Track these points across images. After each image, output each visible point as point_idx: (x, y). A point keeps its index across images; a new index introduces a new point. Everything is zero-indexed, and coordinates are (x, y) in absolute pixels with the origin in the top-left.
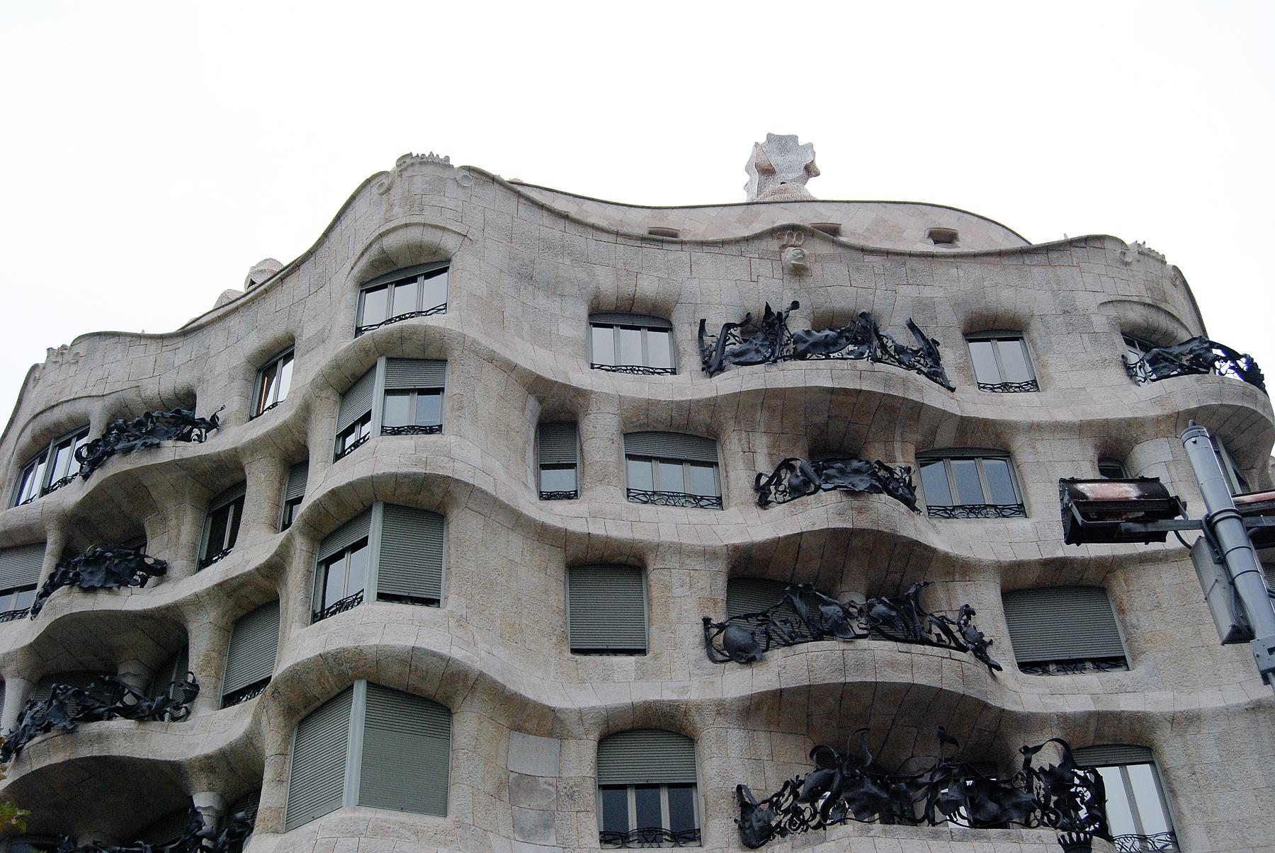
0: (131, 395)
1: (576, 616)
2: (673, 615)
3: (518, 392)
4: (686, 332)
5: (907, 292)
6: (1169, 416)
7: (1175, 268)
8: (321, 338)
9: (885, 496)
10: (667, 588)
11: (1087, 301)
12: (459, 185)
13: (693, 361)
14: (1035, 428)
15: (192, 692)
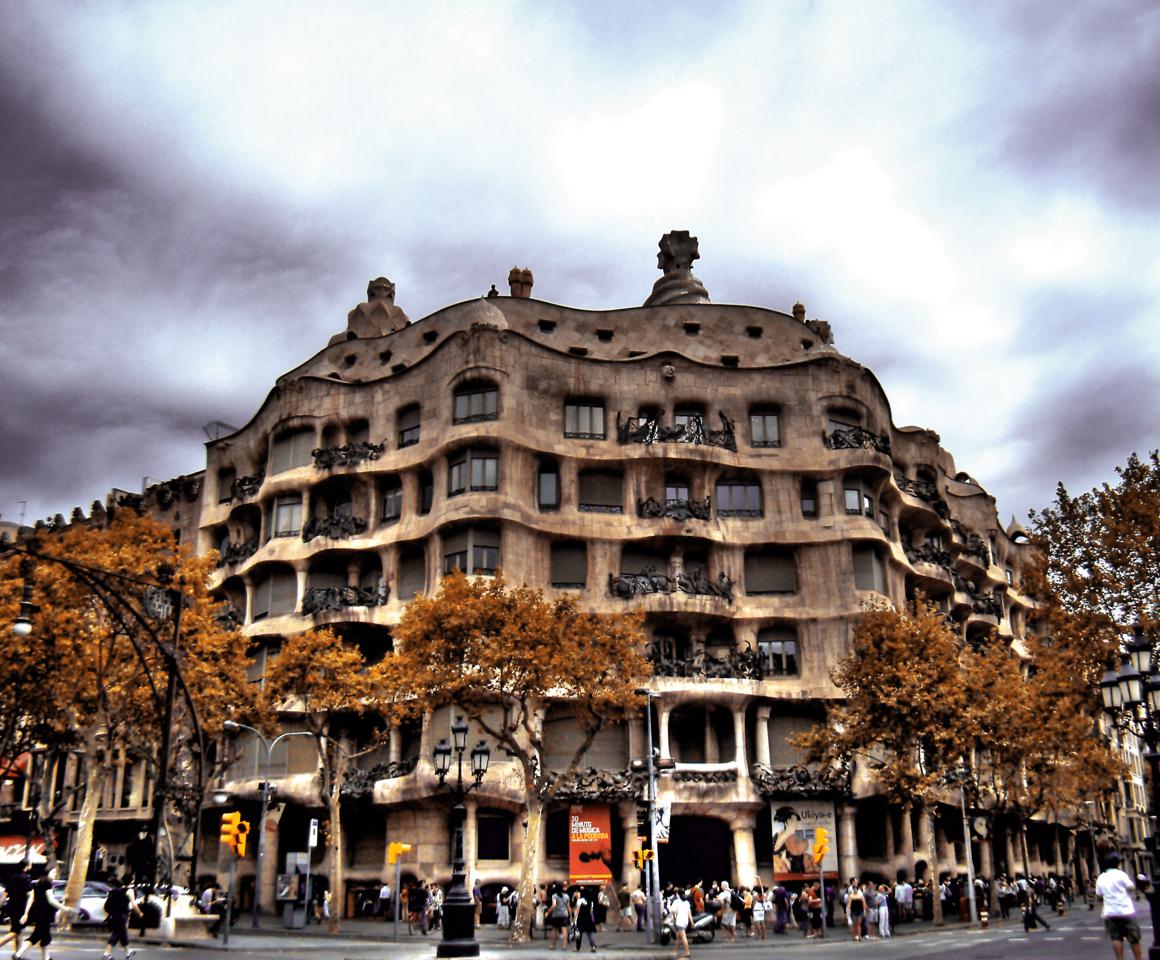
0: (334, 417)
1: (554, 569)
2: (597, 571)
3: (530, 459)
4: (612, 415)
5: (721, 390)
6: (834, 471)
7: (867, 370)
8: (434, 414)
9: (694, 520)
10: (594, 558)
11: (813, 396)
12: (501, 341)
13: (613, 434)
14: (772, 473)
15: (388, 591)
